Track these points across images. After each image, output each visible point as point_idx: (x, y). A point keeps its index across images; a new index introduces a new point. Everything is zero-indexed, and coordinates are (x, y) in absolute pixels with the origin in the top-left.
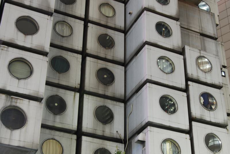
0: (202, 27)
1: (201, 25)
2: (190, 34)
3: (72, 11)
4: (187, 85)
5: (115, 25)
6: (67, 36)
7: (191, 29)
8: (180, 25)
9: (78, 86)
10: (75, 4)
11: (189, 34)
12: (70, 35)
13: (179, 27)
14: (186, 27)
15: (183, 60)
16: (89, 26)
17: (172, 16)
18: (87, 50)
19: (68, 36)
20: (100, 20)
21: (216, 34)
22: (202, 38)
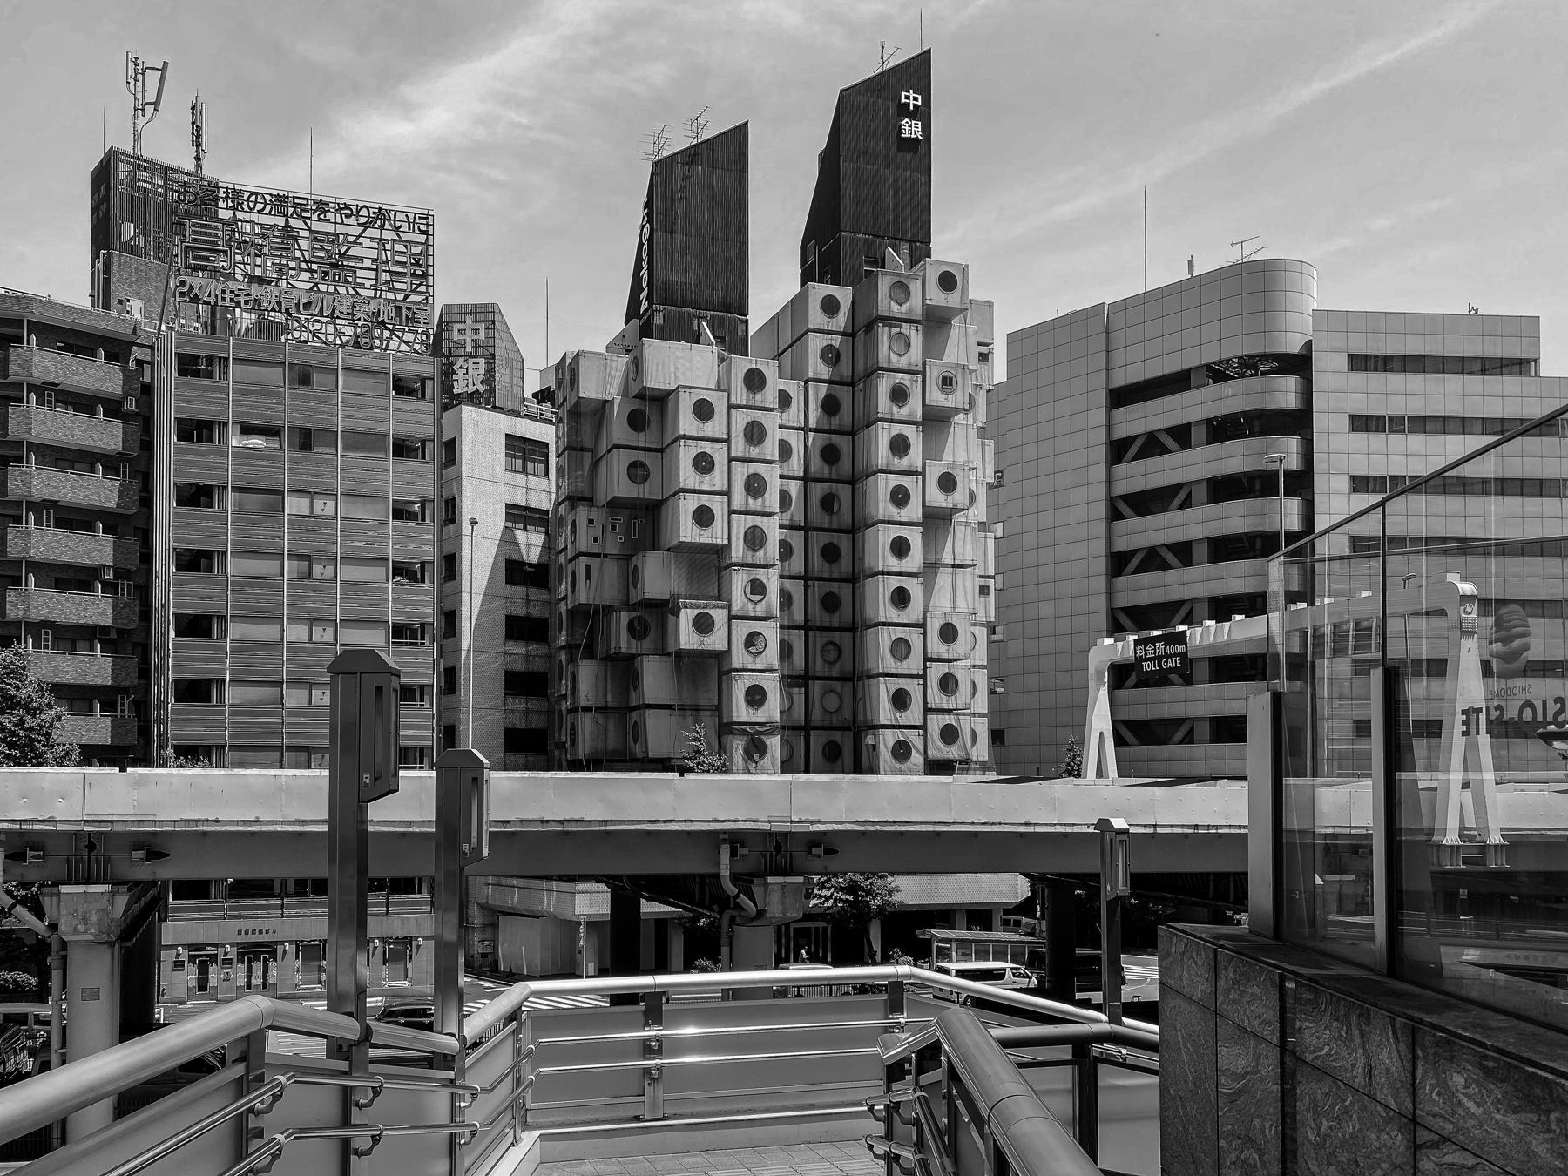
4: (925, 669)
9: (802, 673)
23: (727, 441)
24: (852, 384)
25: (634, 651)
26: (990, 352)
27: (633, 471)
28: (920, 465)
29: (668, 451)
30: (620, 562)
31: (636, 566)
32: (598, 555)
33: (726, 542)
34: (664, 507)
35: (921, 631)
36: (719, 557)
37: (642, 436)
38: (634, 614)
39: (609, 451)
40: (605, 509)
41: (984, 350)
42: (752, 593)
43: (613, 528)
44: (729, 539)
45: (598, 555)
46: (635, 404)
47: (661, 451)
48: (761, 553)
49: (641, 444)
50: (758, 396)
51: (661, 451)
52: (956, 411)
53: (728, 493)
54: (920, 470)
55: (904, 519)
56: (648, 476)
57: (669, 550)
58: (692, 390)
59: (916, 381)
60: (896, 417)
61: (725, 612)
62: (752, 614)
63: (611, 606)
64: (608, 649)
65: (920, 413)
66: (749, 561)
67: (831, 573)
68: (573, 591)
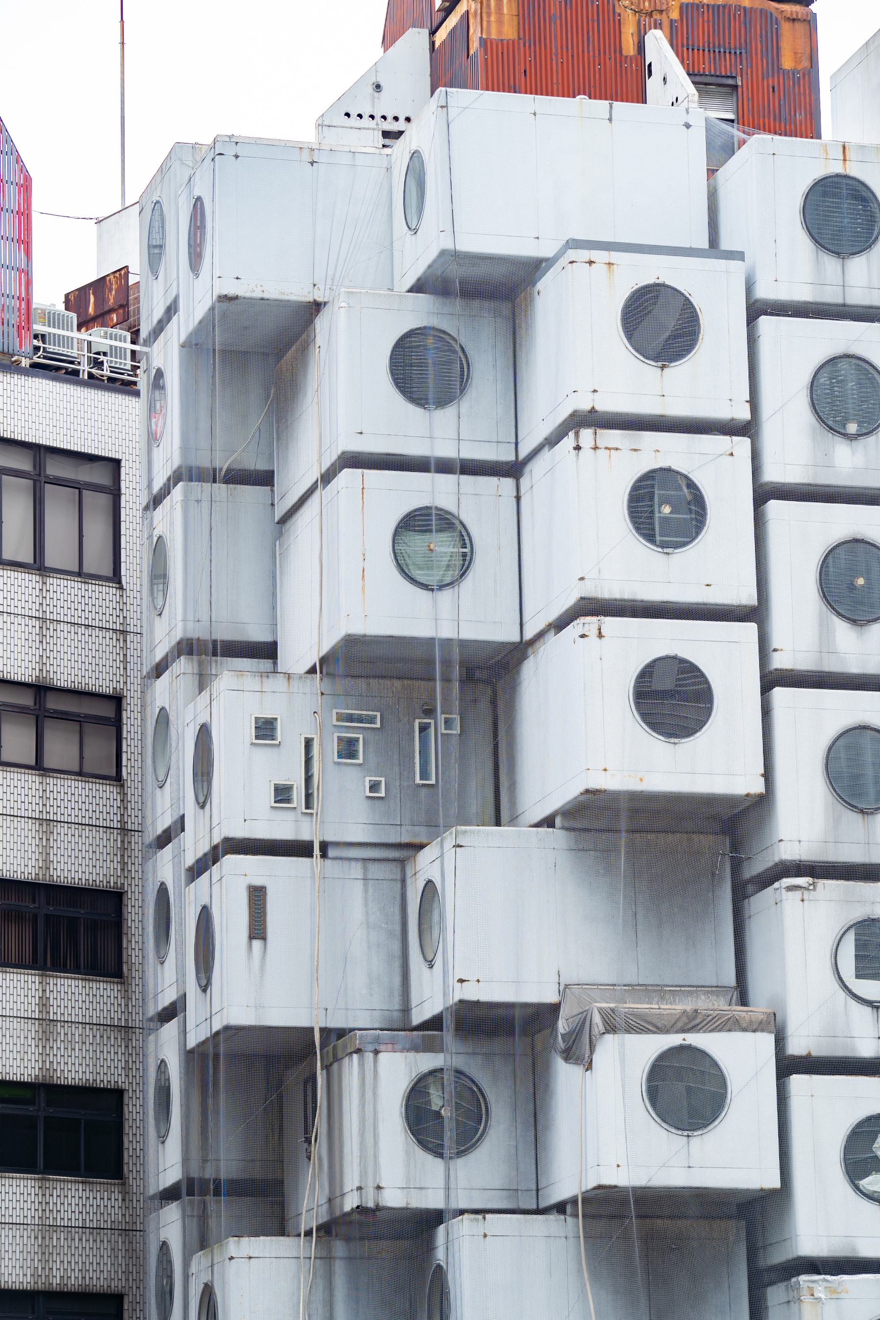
25: (433, 1201)
27: (416, 542)
29: (536, 470)
30: (376, 870)
31: (429, 883)
32: (301, 849)
33: (757, 787)
34: (529, 669)
36: (735, 847)
37: (445, 417)
38: (428, 1062)
39: (327, 477)
42: (858, 976)
43: (348, 749)
44: (768, 775)
45: (301, 849)
49: (446, 450)
56: (466, 563)
57: (548, 822)
58: (615, 256)
61: (768, 1040)
68: (205, 988)
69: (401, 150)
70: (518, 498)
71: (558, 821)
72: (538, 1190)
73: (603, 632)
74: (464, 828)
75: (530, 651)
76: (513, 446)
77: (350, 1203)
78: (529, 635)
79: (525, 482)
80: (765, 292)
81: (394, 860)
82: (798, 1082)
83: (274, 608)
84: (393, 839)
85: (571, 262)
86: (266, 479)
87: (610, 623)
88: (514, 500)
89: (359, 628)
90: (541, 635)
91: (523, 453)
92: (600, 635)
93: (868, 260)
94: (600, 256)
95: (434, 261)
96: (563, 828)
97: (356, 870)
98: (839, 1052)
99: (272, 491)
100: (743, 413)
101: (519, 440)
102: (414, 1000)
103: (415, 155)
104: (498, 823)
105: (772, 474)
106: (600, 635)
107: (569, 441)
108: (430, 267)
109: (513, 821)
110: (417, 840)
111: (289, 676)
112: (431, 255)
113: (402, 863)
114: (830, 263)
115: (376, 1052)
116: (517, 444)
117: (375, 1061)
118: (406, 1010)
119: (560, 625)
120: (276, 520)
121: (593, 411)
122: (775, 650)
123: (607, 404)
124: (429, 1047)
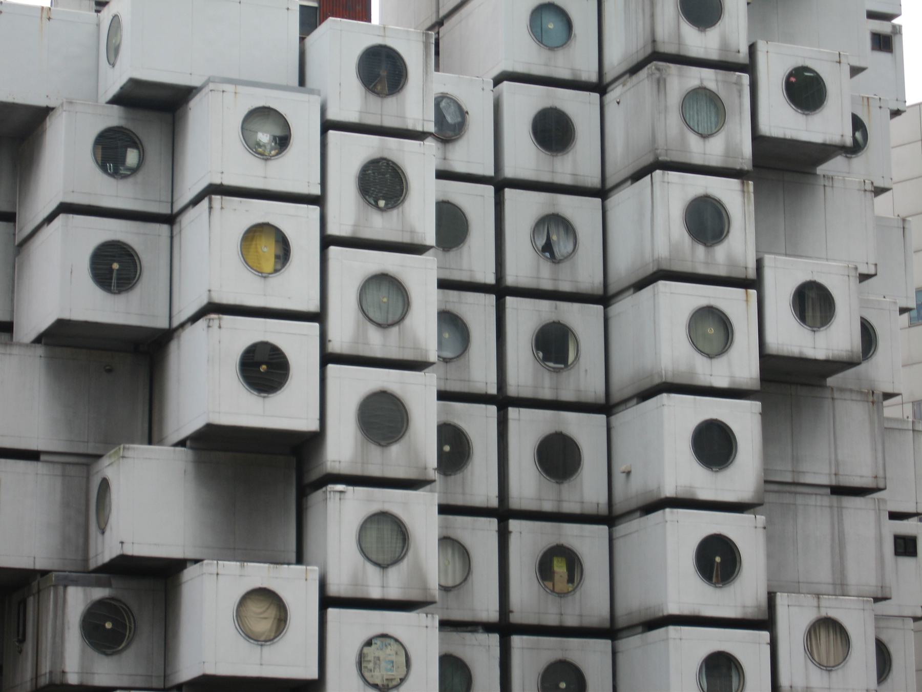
0: (837, 461)
1: (836, 455)
2: (800, 500)
3: (464, 494)
5: (582, 502)
6: (458, 582)
7: (802, 481)
8: (765, 528)
10: (469, 467)
11: (795, 504)
12: (465, 580)
13: (760, 536)
14: (789, 479)
15: (768, 648)
16: (510, 532)
17: (743, 501)
18: (511, 615)
19: (461, 584)
20: (540, 500)
21: (881, 474)
22: (835, 504)
23: (318, 201)
24: (600, 88)
26: (897, 30)
28: (752, 265)
34: (173, 346)
35: (765, 635)
38: (99, 593)
40: (40, 350)
41: (882, 27)
46: (114, 117)
47: (170, 219)
48: (395, 449)
50: (391, 103)
51: (170, 219)
52: (826, 152)
53: (319, 317)
54: (752, 274)
55: (721, 382)
57: (182, 443)
58: (240, 89)
59: (739, 83)
60: (697, 160)
62: (375, 593)
63: (44, 573)
64: (37, 676)
65: (747, 148)
66: (374, 471)
67: (560, 501)
69: (107, 14)
70: (172, 238)
71: (188, 443)
72: (165, 677)
73: (222, 326)
74: (127, 446)
75: (176, 335)
76: (170, 204)
77: (44, 681)
78: (176, 323)
79: (176, 228)
80: (332, 115)
81: (83, 464)
82: (332, 612)
83: (12, 300)
84: (82, 450)
85: (211, 91)
86: (10, 217)
87: (227, 319)
88: (168, 240)
89: (66, 316)
90: (182, 326)
91: (177, 208)
92: (220, 327)
93: (397, 98)
94: (229, 88)
95: (125, 85)
96: (192, 448)
97: (58, 470)
98: (359, 595)
99: (15, 226)
100: (316, 191)
101: (175, 198)
102: (92, 553)
103: (116, 19)
104: (150, 442)
105: (334, 229)
106: (220, 327)
107: (205, 203)
108: (122, 88)
109: (161, 442)
110: (99, 452)
111: (20, 345)
112: (123, 80)
113: (88, 466)
114: (373, 100)
115: (65, 587)
116: (172, 203)
117: (65, 592)
118: (86, 560)
119: (194, 319)
120: (17, 243)
121: (221, 185)
122: (330, 341)
123: (230, 180)
124: (99, 584)
